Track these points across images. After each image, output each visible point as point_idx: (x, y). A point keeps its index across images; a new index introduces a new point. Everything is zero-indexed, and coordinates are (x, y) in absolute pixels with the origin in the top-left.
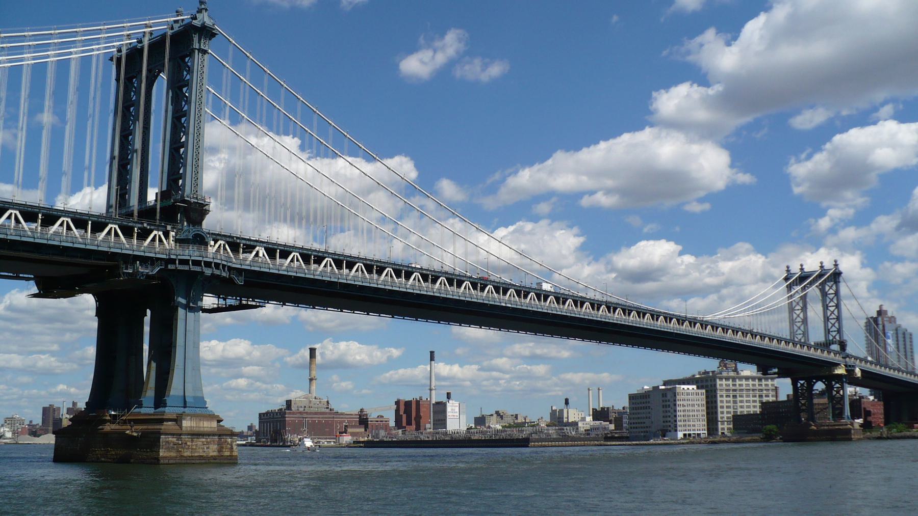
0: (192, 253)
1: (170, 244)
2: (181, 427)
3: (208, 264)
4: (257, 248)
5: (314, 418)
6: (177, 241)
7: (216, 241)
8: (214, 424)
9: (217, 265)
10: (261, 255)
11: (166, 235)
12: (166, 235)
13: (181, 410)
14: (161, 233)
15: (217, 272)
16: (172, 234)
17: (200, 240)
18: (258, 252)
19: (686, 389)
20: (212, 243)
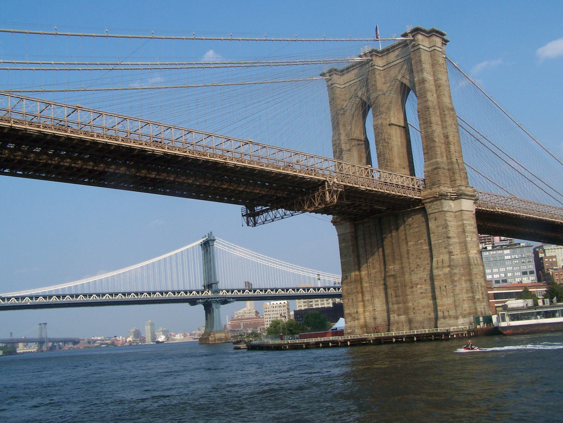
1: (210, 293)
3: (218, 298)
7: (222, 291)
9: (220, 298)
12: (208, 291)
14: (207, 292)
15: (220, 299)
17: (217, 291)
20: (221, 292)
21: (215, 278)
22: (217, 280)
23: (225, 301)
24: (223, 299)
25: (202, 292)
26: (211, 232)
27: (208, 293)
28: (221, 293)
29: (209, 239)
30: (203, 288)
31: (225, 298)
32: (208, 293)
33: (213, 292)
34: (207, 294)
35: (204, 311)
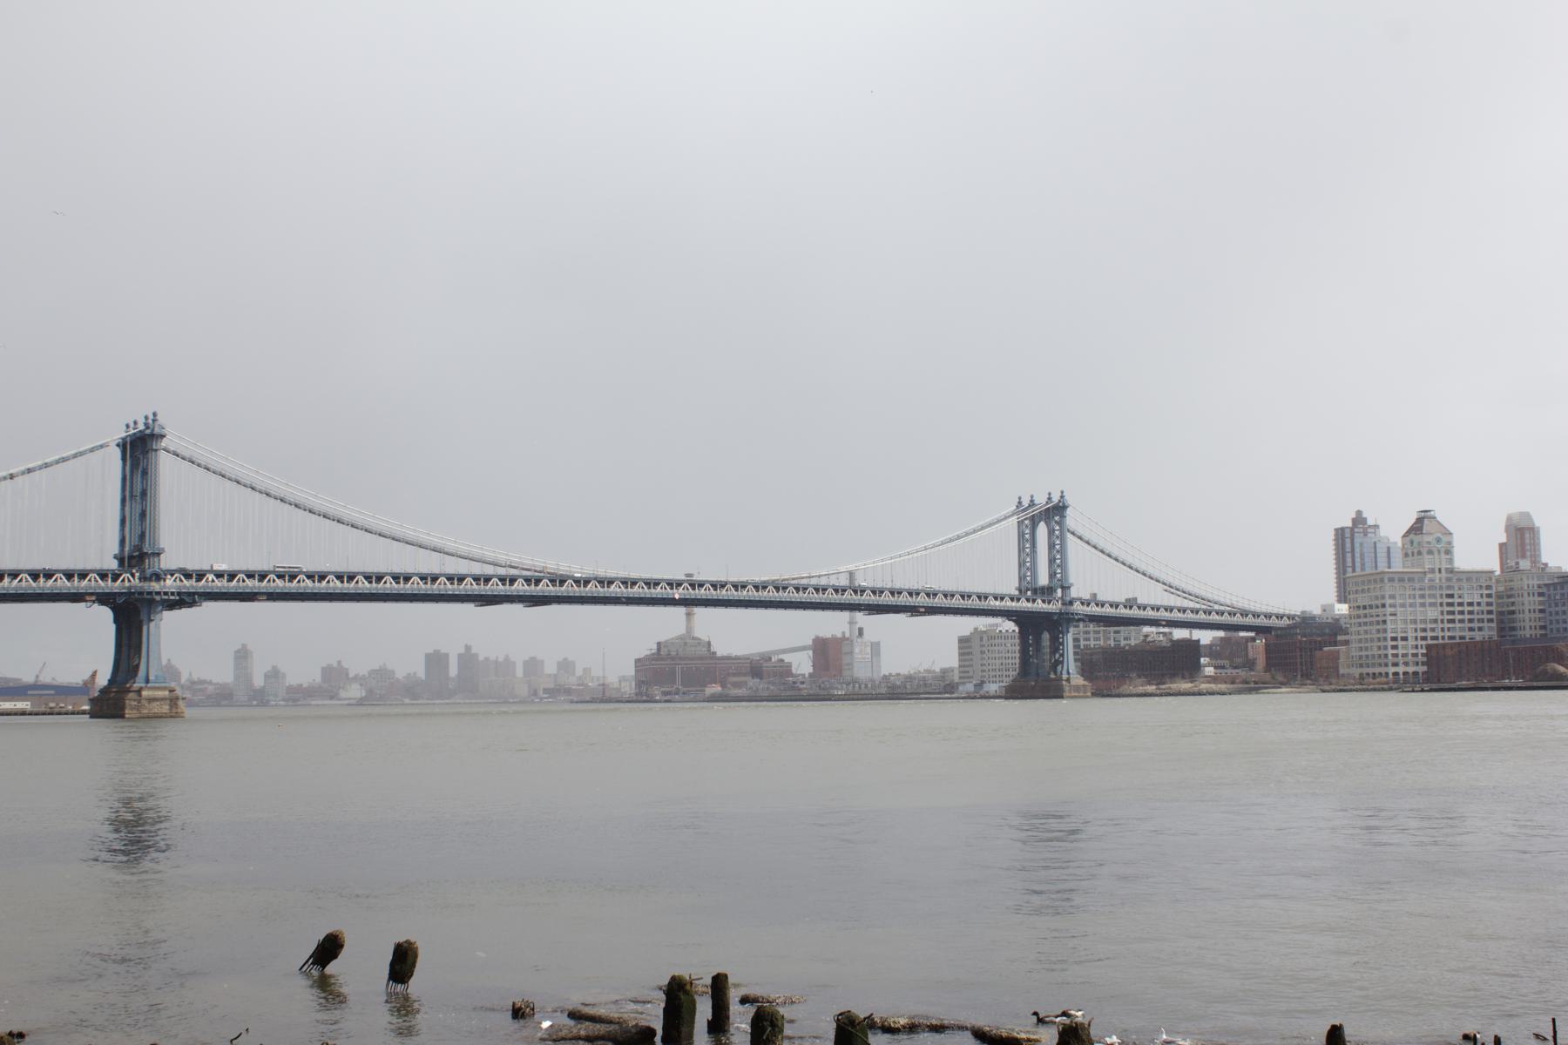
0: (155, 586)
2: (140, 696)
4: (208, 575)
5: (691, 664)
6: (140, 579)
7: (172, 575)
8: (167, 693)
10: (210, 579)
11: (133, 576)
13: (143, 685)
14: (128, 575)
15: (166, 597)
16: (137, 574)
18: (208, 578)
19: (1004, 631)
20: (169, 577)
21: (154, 542)
22: (161, 546)
23: (184, 600)
24: (172, 598)
25: (115, 577)
26: (155, 414)
27: (131, 579)
28: (169, 581)
29: (148, 432)
30: (114, 565)
31: (179, 594)
32: (131, 579)
33: (143, 579)
34: (129, 581)
35: (113, 627)
